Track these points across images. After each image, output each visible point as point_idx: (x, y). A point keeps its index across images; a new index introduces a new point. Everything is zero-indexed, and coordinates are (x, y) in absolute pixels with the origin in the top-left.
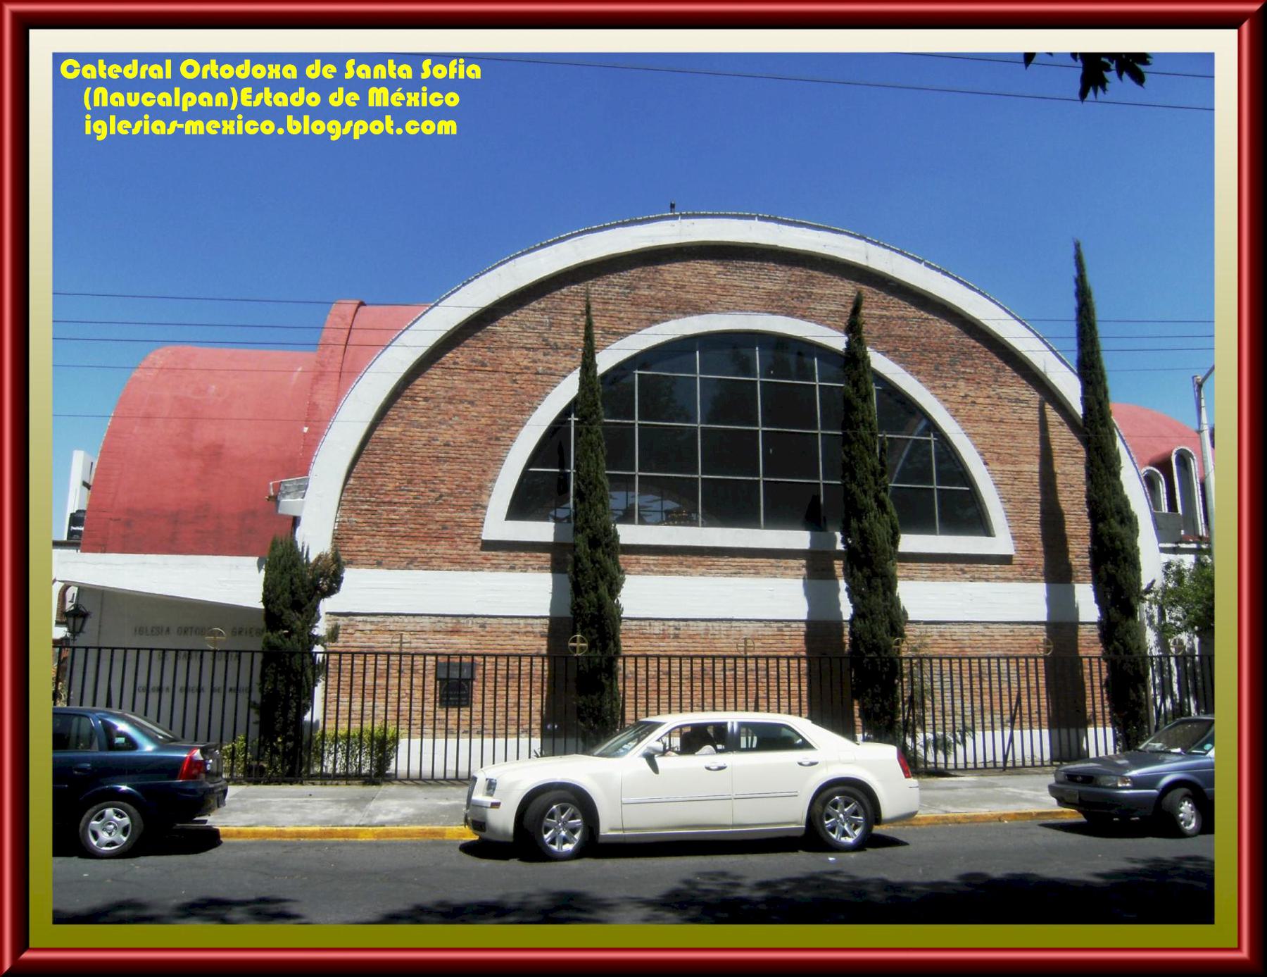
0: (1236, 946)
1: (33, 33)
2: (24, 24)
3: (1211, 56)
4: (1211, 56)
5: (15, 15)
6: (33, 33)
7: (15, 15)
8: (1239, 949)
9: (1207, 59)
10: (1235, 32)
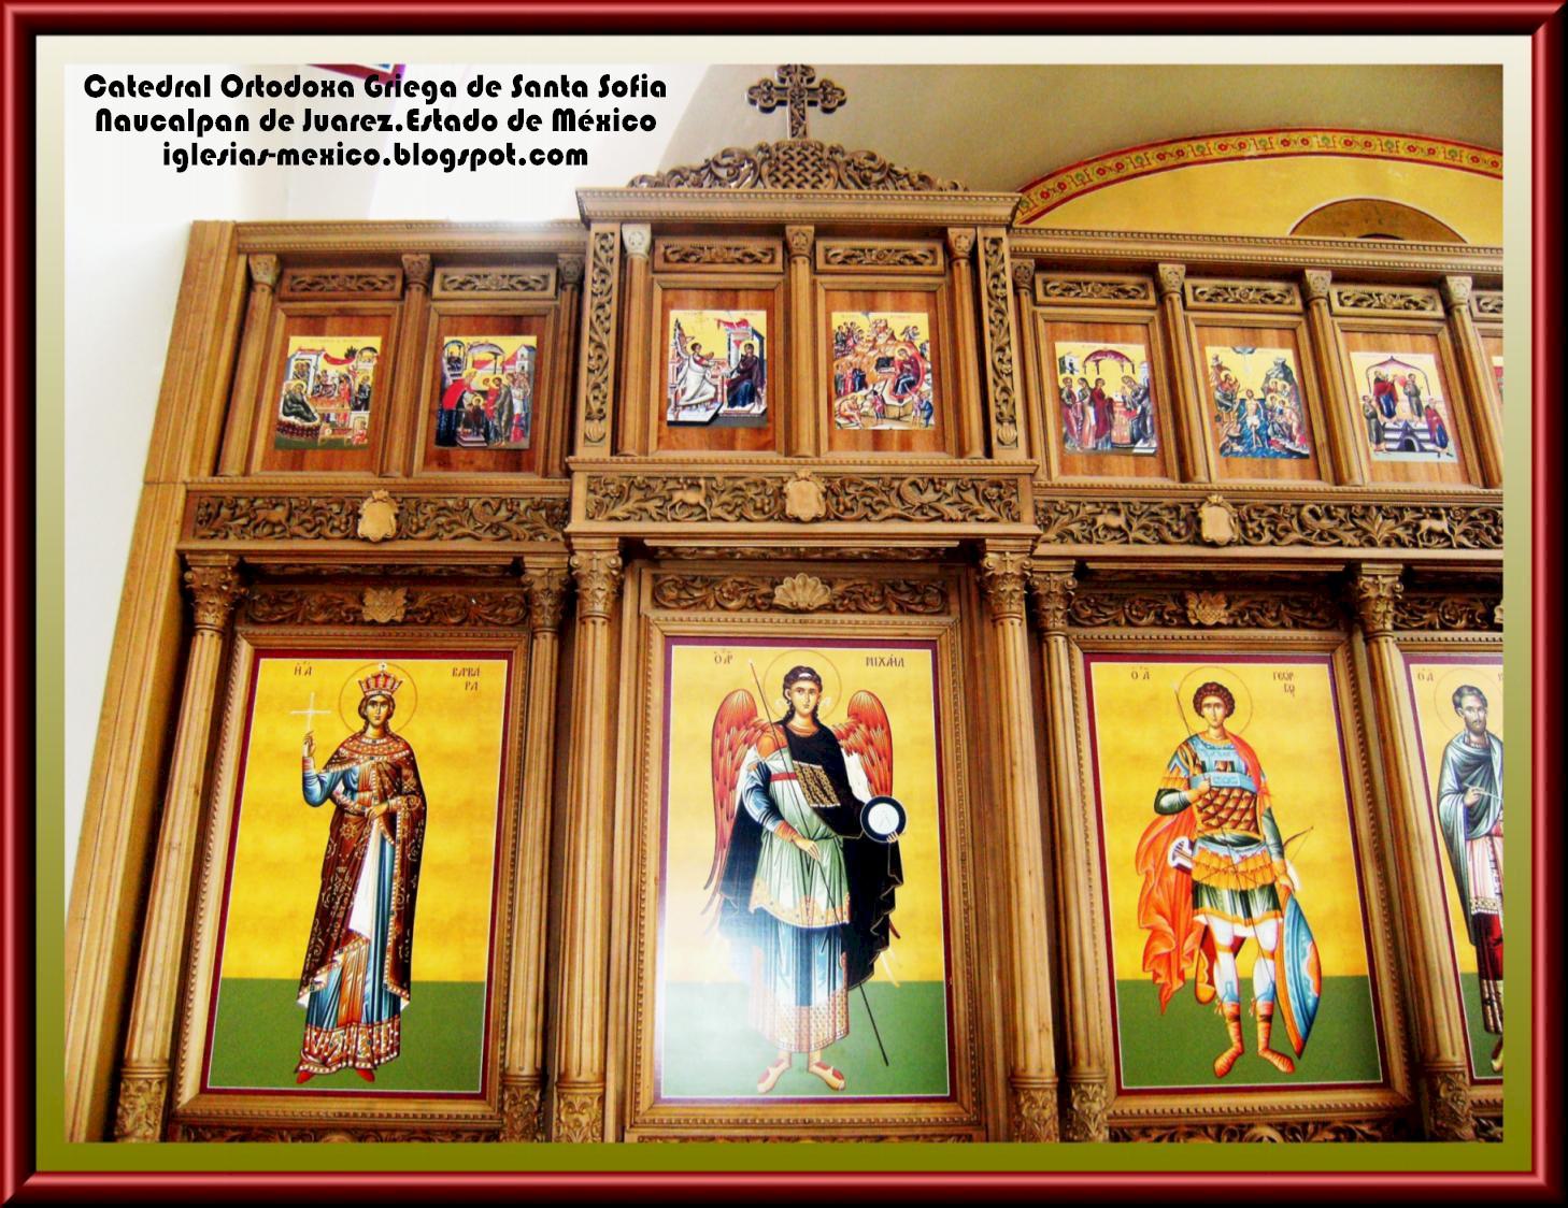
0: (1529, 1169)
1: (43, 42)
2: (31, 29)
3: (1500, 67)
4: (1500, 67)
5: (18, 18)
6: (43, 42)
7: (18, 18)
8: (1533, 1172)
9: (1493, 74)
10: (1527, 39)
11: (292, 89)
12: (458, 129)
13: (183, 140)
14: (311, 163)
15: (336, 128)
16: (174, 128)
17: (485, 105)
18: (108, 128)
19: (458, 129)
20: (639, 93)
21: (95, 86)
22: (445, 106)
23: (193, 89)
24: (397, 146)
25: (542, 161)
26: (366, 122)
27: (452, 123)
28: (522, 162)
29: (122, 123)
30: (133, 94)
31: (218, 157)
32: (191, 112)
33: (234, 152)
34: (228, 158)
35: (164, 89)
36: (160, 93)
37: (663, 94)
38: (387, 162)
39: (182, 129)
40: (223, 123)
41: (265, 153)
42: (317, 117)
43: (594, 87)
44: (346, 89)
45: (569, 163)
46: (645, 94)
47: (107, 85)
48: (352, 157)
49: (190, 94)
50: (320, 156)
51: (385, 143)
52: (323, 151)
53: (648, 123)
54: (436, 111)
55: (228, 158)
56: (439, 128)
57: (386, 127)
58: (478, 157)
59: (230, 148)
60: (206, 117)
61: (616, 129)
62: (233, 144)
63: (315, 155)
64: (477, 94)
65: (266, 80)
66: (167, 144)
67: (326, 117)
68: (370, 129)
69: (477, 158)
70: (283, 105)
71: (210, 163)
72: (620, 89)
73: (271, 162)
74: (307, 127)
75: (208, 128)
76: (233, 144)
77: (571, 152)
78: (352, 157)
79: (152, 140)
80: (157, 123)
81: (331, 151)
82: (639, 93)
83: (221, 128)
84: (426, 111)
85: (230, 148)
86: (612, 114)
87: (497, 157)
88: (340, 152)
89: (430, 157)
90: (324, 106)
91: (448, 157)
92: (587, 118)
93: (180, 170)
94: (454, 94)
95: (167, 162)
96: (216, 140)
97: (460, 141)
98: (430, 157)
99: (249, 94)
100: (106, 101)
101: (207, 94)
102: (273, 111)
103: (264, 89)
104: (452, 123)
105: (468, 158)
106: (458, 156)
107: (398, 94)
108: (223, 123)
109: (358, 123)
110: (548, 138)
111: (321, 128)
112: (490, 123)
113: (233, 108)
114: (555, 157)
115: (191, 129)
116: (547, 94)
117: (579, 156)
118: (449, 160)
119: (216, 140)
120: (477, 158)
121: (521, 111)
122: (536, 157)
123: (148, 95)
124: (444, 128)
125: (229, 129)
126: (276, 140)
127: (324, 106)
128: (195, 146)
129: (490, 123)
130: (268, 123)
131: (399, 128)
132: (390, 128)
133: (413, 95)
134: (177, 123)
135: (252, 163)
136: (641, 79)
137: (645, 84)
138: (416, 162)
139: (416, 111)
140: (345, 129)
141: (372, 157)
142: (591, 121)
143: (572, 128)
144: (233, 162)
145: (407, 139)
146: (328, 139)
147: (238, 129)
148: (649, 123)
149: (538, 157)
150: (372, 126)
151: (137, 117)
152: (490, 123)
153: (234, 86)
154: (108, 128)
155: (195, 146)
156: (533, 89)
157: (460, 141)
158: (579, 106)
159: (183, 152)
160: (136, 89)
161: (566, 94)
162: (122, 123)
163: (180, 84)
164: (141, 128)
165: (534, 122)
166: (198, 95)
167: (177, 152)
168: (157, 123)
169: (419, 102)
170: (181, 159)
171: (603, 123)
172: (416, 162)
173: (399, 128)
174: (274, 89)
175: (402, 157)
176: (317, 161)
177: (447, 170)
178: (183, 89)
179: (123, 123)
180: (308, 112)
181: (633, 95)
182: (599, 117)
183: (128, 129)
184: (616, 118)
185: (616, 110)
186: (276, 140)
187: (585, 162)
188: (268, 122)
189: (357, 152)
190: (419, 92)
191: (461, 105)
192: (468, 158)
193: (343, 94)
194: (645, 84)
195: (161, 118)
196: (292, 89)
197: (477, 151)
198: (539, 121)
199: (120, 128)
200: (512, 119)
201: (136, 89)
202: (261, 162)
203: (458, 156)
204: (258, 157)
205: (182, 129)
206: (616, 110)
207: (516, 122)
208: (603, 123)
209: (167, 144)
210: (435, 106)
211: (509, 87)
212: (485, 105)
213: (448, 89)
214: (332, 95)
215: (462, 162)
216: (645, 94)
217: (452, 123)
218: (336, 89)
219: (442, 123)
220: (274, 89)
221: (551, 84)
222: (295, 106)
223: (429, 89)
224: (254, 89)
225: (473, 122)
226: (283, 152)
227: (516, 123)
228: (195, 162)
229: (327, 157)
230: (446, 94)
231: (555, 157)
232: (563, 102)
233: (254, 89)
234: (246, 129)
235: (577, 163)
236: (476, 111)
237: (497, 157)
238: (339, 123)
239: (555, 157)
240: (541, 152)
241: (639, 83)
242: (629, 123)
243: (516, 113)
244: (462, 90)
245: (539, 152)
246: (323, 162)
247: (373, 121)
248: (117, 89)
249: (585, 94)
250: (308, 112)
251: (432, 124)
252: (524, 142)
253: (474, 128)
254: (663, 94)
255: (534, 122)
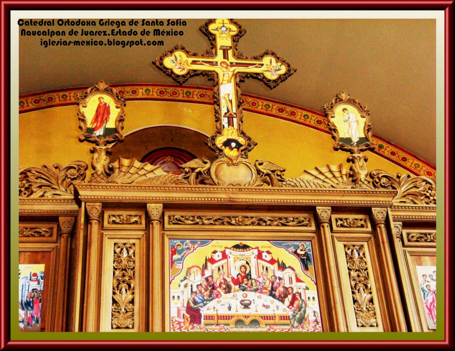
11: (78, 23)
12: (126, 35)
13: (46, 38)
14: (83, 45)
15: (91, 35)
16: (44, 35)
17: (134, 28)
18: (25, 35)
19: (126, 35)
20: (179, 24)
21: (21, 22)
22: (123, 28)
23: (49, 23)
24: (108, 40)
25: (150, 44)
26: (99, 33)
27: (124, 33)
28: (145, 44)
29: (29, 33)
30: (32, 25)
31: (57, 43)
32: (49, 30)
33: (61, 42)
34: (59, 43)
35: (41, 23)
36: (40, 25)
37: (186, 25)
38: (105, 45)
39: (46, 35)
40: (58, 33)
41: (70, 42)
42: (85, 32)
43: (166, 23)
44: (93, 23)
45: (158, 45)
46: (180, 25)
47: (24, 22)
48: (95, 43)
49: (48, 25)
50: (86, 43)
51: (105, 39)
52: (87, 41)
53: (181, 33)
54: (120, 30)
55: (59, 43)
56: (120, 35)
57: (105, 34)
58: (132, 43)
59: (60, 40)
60: (53, 32)
61: (172, 35)
62: (61, 39)
63: (84, 43)
64: (132, 25)
65: (70, 21)
66: (42, 39)
67: (88, 32)
68: (100, 35)
69: (132, 43)
70: (75, 28)
71: (54, 45)
72: (173, 23)
73: (72, 45)
74: (82, 35)
75: (54, 35)
76: (61, 39)
77: (159, 42)
78: (95, 43)
79: (38, 38)
80: (39, 33)
81: (89, 41)
82: (179, 24)
83: (57, 35)
84: (117, 30)
85: (60, 40)
86: (171, 31)
87: (137, 43)
88: (92, 42)
89: (118, 43)
90: (87, 28)
91: (123, 43)
92: (163, 32)
93: (45, 47)
94: (125, 25)
95: (41, 45)
96: (56, 38)
97: (127, 38)
98: (118, 43)
99: (65, 25)
100: (24, 27)
101: (53, 25)
102: (72, 30)
103: (70, 23)
104: (124, 33)
105: (129, 44)
106: (126, 43)
107: (109, 25)
108: (58, 33)
109: (97, 33)
110: (152, 38)
111: (86, 35)
112: (135, 33)
113: (61, 29)
114: (154, 43)
115: (49, 35)
116: (152, 25)
117: (161, 43)
118: (123, 44)
119: (56, 38)
120: (132, 43)
121: (144, 30)
122: (149, 43)
123: (36, 25)
124: (122, 35)
125: (60, 35)
126: (73, 38)
127: (87, 28)
128: (50, 40)
129: (135, 33)
130: (71, 33)
131: (109, 35)
132: (106, 35)
133: (113, 25)
134: (44, 33)
135: (66, 45)
136: (179, 20)
137: (180, 22)
138: (114, 45)
139: (114, 30)
140: (93, 35)
141: (101, 43)
142: (165, 33)
143: (159, 35)
144: (61, 45)
145: (111, 38)
146: (88, 38)
147: (62, 35)
148: (181, 33)
149: (149, 43)
150: (101, 34)
151: (33, 32)
152: (135, 33)
153: (61, 22)
154: (25, 35)
155: (50, 40)
156: (148, 23)
157: (127, 38)
158: (161, 28)
159: (46, 42)
160: (33, 23)
161: (157, 25)
162: (29, 33)
163: (45, 22)
164: (34, 35)
165: (148, 33)
166: (51, 25)
167: (45, 42)
168: (39, 33)
169: (115, 27)
170: (46, 44)
171: (168, 33)
172: (114, 45)
173: (109, 35)
174: (73, 23)
175: (110, 43)
176: (85, 44)
177: (123, 47)
178: (46, 24)
179: (29, 33)
180: (83, 30)
181: (177, 25)
182: (167, 32)
183: (30, 35)
184: (172, 32)
185: (172, 29)
186: (73, 38)
187: (163, 45)
188: (71, 33)
189: (97, 42)
190: (115, 24)
191: (127, 28)
192: (129, 44)
193: (93, 25)
194: (180, 22)
195: (40, 32)
196: (78, 23)
197: (132, 42)
198: (150, 33)
199: (28, 35)
200: (142, 32)
201: (33, 23)
202: (69, 44)
203: (126, 43)
204: (68, 43)
205: (46, 35)
206: (172, 29)
207: (143, 33)
208: (168, 33)
209: (42, 39)
210: (119, 28)
211: (141, 23)
212: (134, 28)
213: (123, 23)
214: (90, 25)
215: (127, 44)
216: (180, 25)
217: (124, 33)
218: (91, 23)
219: (121, 33)
220: (73, 23)
221: (153, 22)
222: (79, 28)
223: (118, 23)
224: (67, 24)
225: (130, 33)
226: (75, 42)
227: (143, 33)
228: (50, 45)
229: (88, 43)
230: (122, 25)
231: (154, 43)
232: (156, 27)
233: (67, 24)
234: (65, 35)
235: (161, 45)
236: (131, 30)
237: (137, 43)
238: (92, 33)
239: (154, 43)
240: (150, 42)
241: (179, 22)
242: (176, 33)
243: (143, 30)
244: (127, 23)
245: (149, 42)
246: (87, 45)
247: (101, 33)
248: (27, 23)
249: (163, 25)
250: (83, 30)
251: (118, 33)
252: (146, 39)
253: (131, 35)
254: (186, 25)
255: (148, 33)
